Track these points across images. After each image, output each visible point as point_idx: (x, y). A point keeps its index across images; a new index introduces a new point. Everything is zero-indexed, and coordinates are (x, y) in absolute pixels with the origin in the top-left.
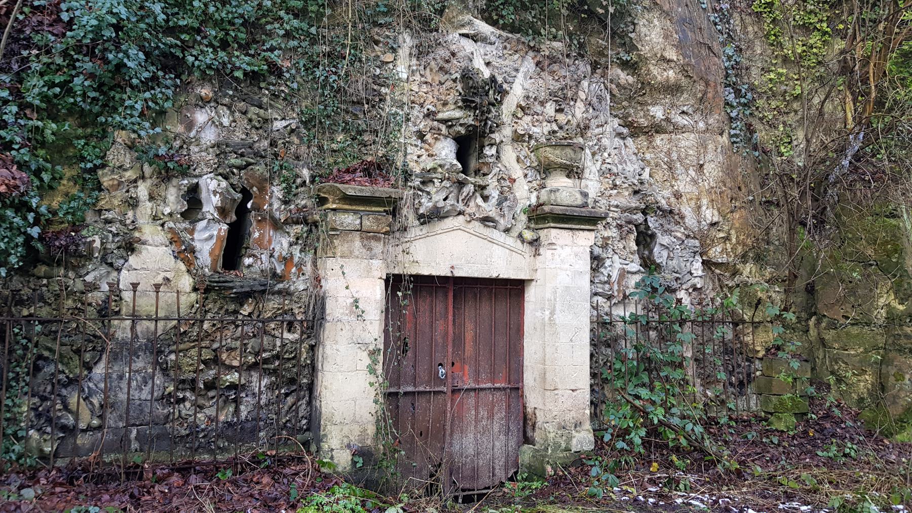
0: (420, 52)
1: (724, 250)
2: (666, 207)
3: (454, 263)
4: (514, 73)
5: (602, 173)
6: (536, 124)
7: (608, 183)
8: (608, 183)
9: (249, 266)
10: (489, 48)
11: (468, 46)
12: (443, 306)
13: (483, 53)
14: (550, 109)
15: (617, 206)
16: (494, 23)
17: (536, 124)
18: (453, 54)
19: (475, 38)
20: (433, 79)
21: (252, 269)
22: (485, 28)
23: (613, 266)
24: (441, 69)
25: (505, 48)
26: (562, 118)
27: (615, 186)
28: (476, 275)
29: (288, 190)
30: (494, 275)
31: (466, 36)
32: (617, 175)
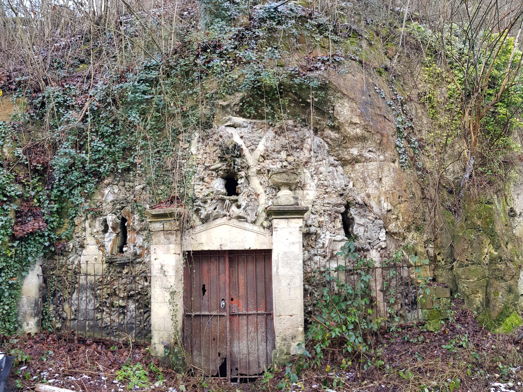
0: (203, 139)
1: (396, 225)
2: (361, 202)
3: (223, 242)
4: (259, 139)
5: (318, 186)
6: (273, 163)
7: (322, 191)
8: (322, 191)
9: (126, 251)
10: (243, 129)
11: (231, 130)
12: (224, 266)
13: (239, 132)
14: (283, 155)
15: (329, 204)
16: (244, 116)
17: (273, 163)
18: (221, 136)
19: (234, 126)
20: (210, 151)
21: (128, 253)
22: (239, 120)
23: (326, 238)
24: (214, 144)
25: (253, 128)
26: (291, 159)
27: (327, 193)
28: (236, 249)
29: (141, 215)
30: (247, 248)
31: (227, 126)
32: (327, 186)
